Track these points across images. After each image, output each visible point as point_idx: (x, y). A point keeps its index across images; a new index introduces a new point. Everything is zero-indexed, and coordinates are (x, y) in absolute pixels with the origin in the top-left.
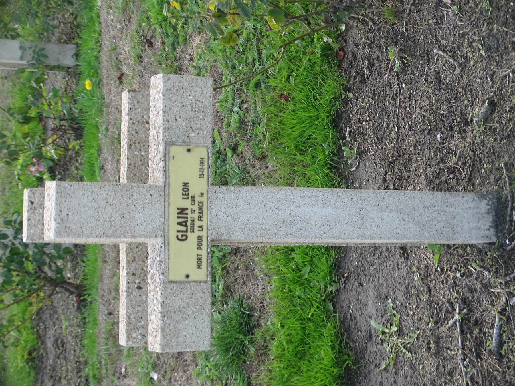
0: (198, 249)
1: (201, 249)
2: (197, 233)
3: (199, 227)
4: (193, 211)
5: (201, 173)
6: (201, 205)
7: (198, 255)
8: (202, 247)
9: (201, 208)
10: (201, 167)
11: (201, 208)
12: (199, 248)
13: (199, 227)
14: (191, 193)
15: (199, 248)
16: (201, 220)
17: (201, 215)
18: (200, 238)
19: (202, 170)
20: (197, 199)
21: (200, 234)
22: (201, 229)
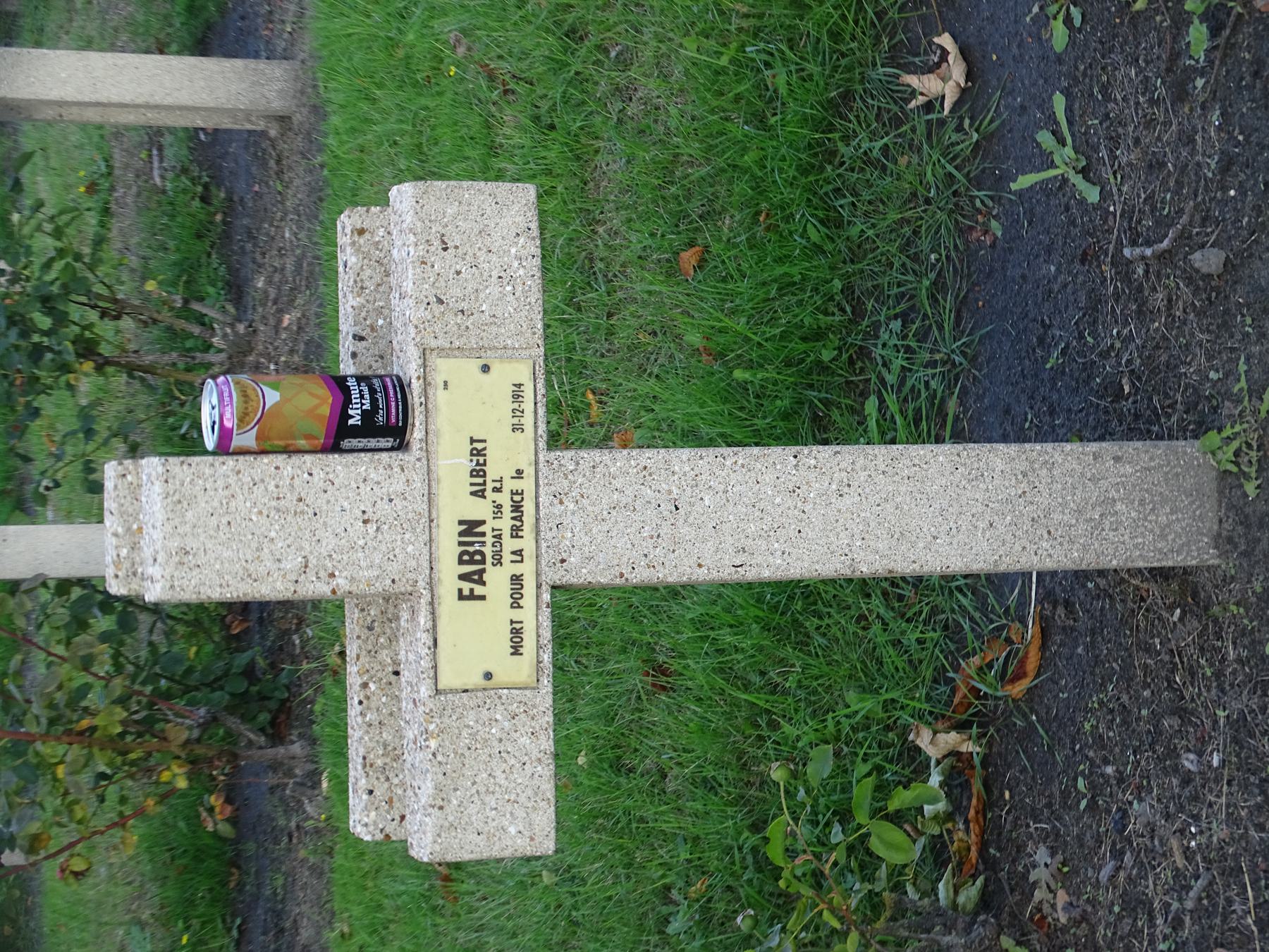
1: (520, 607)
2: (508, 569)
3: (513, 553)
5: (516, 421)
6: (517, 498)
7: (512, 622)
9: (517, 507)
10: (516, 406)
11: (517, 507)
12: (516, 605)
13: (513, 553)
14: (492, 472)
15: (516, 605)
16: (517, 536)
17: (518, 524)
18: (517, 579)
19: (518, 414)
20: (509, 485)
21: (517, 569)
22: (519, 558)
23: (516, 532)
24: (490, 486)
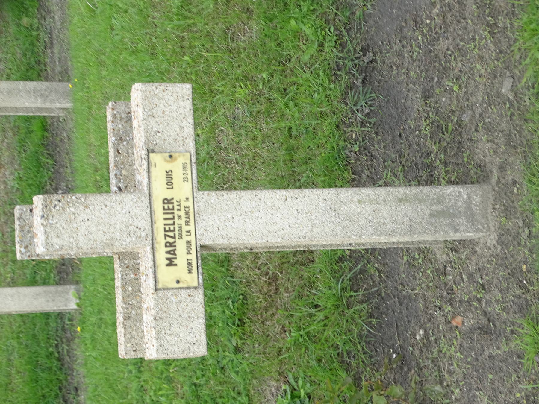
0: (187, 254)
2: (186, 238)
3: (187, 232)
4: (180, 217)
6: (187, 209)
8: (191, 252)
9: (187, 213)
10: (184, 172)
11: (187, 213)
12: (189, 253)
13: (187, 232)
15: (189, 253)
17: (188, 220)
18: (189, 242)
20: (183, 204)
21: (189, 238)
22: (189, 234)
23: (187, 223)
24: (176, 204)
